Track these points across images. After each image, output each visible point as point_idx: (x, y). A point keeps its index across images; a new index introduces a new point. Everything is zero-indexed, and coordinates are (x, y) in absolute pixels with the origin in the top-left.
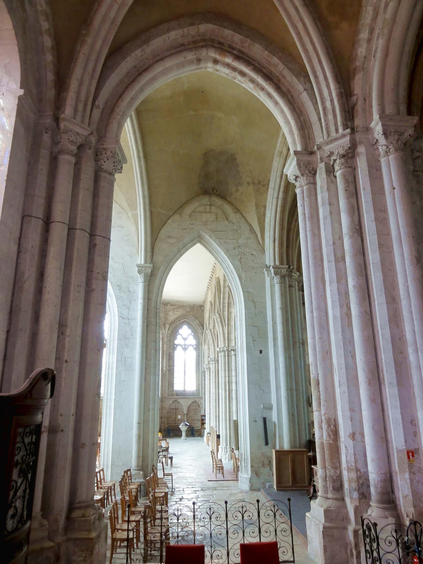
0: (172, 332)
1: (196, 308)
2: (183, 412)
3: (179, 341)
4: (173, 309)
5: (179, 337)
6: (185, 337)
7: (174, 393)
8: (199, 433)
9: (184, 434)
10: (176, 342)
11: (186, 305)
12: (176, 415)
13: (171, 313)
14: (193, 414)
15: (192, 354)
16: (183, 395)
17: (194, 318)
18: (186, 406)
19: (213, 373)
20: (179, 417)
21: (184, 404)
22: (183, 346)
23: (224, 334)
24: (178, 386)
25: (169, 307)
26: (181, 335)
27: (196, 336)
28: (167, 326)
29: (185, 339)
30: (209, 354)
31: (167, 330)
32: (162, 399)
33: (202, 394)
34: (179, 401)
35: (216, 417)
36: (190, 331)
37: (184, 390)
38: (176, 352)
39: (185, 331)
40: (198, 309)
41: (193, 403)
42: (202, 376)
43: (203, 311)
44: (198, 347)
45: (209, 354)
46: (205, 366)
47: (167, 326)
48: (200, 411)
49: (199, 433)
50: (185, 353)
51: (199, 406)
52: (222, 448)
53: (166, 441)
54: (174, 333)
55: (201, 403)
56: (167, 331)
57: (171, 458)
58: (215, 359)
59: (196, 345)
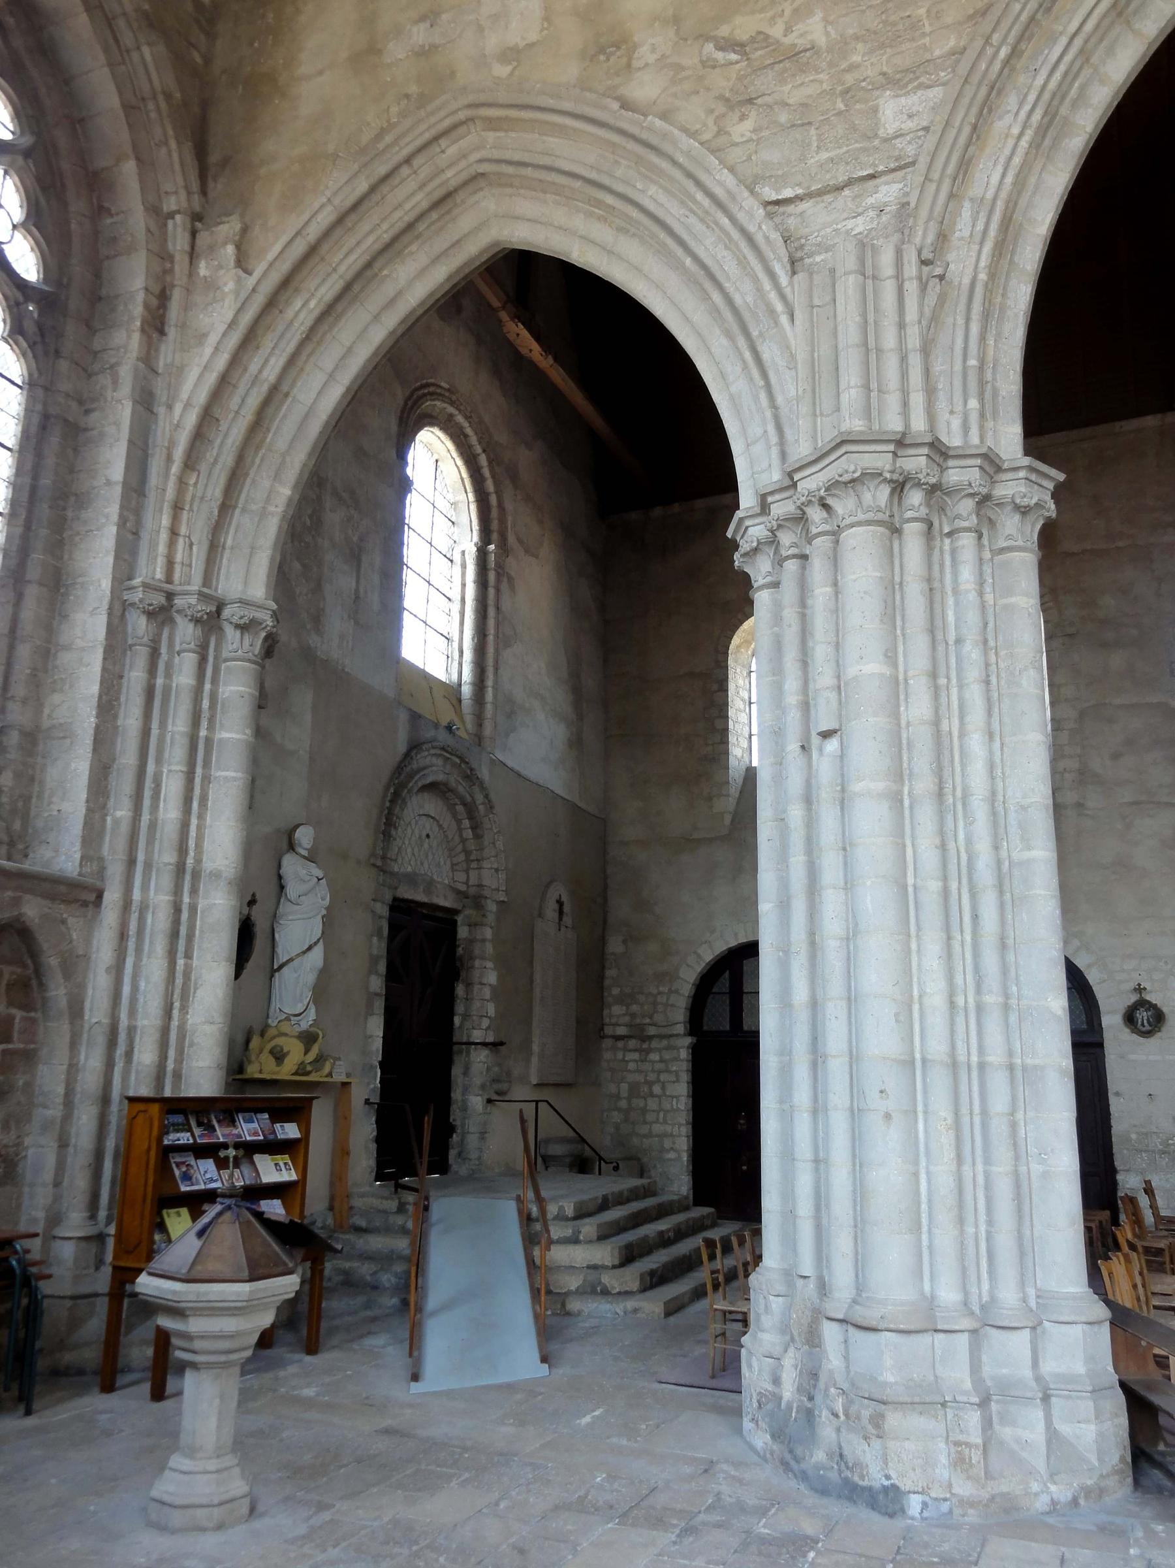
48: (29, 1057)
55: (74, 965)
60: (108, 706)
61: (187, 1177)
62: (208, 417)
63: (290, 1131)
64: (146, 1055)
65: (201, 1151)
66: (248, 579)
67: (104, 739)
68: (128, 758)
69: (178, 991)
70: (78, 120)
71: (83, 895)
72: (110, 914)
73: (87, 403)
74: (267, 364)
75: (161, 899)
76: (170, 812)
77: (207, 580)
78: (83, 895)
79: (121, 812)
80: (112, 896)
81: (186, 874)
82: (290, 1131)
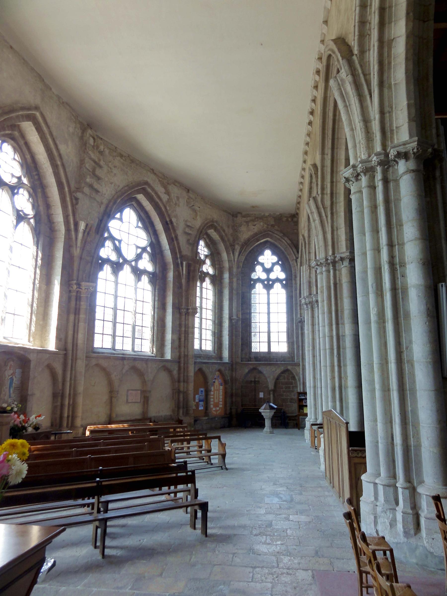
0: (246, 259)
1: (284, 219)
2: (267, 387)
5: (259, 268)
6: (268, 266)
7: (252, 356)
8: (295, 422)
9: (268, 423)
10: (254, 276)
11: (267, 214)
12: (256, 391)
13: (243, 228)
14: (284, 392)
15: (279, 294)
17: (282, 235)
18: (272, 377)
19: (322, 292)
20: (261, 395)
21: (270, 374)
22: (266, 282)
23: (366, 121)
24: (259, 346)
25: (239, 219)
26: (262, 265)
27: (286, 266)
28: (238, 248)
29: (268, 271)
31: (237, 254)
32: (232, 365)
33: (298, 358)
35: (333, 389)
36: (275, 259)
37: (269, 352)
39: (268, 258)
40: (287, 220)
42: (297, 329)
43: (296, 223)
44: (290, 284)
45: (310, 277)
46: (303, 301)
47: (238, 248)
48: (296, 387)
49: (295, 422)
50: (268, 294)
51: (294, 378)
52: (375, 484)
53: (220, 440)
54: (250, 262)
55: (298, 374)
57: (204, 506)
58: (327, 260)
60: (297, 337)
70: (283, 253)
72: (301, 367)
79: (300, 352)
80: (301, 364)
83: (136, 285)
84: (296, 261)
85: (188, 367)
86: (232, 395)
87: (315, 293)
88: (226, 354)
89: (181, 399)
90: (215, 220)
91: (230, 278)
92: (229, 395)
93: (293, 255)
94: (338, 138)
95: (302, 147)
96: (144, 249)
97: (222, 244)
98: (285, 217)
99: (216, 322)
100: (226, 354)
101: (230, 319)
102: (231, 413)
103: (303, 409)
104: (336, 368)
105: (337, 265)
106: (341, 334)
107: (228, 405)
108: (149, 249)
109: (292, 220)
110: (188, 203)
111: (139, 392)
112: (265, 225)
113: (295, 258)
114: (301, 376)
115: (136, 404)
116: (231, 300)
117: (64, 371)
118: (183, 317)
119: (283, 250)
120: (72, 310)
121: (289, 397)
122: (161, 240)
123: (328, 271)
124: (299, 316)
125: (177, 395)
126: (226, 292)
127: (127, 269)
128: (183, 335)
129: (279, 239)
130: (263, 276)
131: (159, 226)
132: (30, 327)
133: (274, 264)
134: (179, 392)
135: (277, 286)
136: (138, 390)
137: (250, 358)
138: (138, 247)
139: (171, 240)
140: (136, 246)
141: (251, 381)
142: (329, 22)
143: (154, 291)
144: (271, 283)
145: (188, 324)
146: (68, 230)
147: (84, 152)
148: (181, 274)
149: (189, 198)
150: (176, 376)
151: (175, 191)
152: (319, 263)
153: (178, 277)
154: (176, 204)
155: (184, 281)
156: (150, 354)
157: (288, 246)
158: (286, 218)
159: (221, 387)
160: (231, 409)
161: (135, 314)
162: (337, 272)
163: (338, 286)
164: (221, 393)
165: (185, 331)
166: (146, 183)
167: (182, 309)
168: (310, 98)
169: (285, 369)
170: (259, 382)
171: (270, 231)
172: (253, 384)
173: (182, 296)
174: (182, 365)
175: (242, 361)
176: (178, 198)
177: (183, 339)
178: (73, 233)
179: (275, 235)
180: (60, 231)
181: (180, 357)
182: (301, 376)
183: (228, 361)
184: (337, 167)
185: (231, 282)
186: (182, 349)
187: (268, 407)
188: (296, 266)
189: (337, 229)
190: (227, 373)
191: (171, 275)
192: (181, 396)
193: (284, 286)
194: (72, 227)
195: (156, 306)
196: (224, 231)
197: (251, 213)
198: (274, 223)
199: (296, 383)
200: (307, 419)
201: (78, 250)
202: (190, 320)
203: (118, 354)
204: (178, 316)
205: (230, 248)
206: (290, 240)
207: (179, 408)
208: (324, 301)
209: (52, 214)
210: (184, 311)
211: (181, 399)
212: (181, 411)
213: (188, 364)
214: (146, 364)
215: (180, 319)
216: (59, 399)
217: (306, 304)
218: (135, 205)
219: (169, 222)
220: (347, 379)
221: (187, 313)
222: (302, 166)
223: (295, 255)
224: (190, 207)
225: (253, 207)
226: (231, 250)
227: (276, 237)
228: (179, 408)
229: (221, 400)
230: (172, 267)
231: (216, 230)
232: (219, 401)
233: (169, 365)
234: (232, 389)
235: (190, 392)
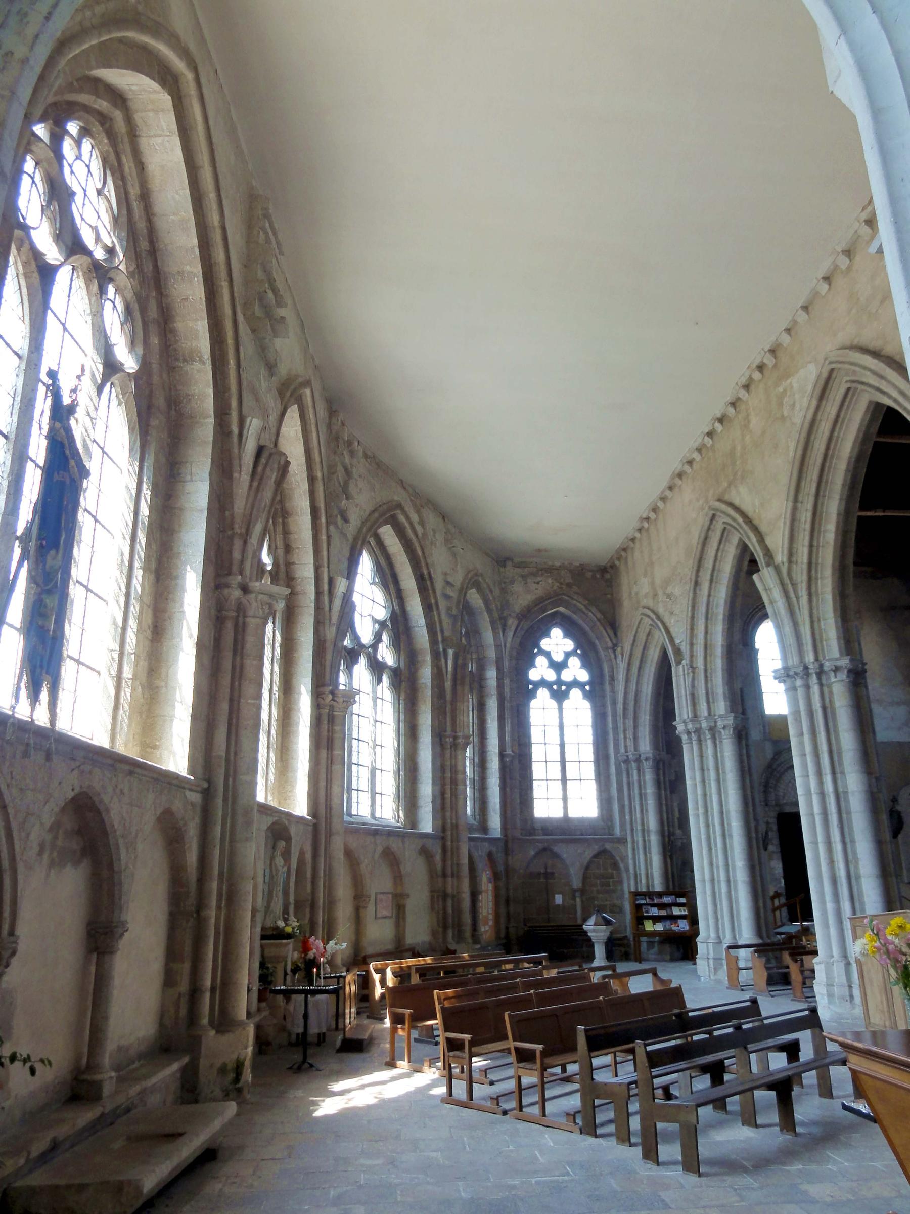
0: (521, 644)
1: (589, 575)
3: (540, 671)
4: (523, 576)
5: (541, 661)
6: (558, 657)
8: (623, 950)
10: (534, 675)
11: (557, 564)
12: (549, 893)
13: (518, 587)
14: (598, 892)
15: (579, 708)
16: (566, 831)
17: (586, 603)
20: (559, 899)
21: (574, 860)
24: (546, 805)
25: (510, 571)
26: (547, 654)
28: (512, 623)
29: (558, 667)
30: (693, 686)
31: (511, 634)
32: (506, 842)
34: (556, 849)
36: (569, 645)
38: (533, 703)
39: (556, 642)
40: (594, 577)
41: (596, 856)
44: (596, 692)
45: (693, 686)
47: (512, 623)
48: (621, 882)
49: (623, 950)
51: (615, 866)
53: (655, 974)
54: (526, 649)
55: (624, 858)
56: (509, 640)
58: (806, 668)
59: (590, 683)
60: (620, 790)
61: (647, 912)
62: (625, 703)
63: (683, 900)
64: (644, 881)
65: (653, 905)
66: (646, 746)
67: (621, 799)
68: (627, 803)
69: (648, 863)
70: (584, 633)
71: (622, 841)
72: (630, 845)
73: (604, 706)
74: (633, 686)
75: (640, 839)
76: (638, 816)
77: (636, 750)
78: (622, 841)
79: (627, 817)
80: (629, 839)
81: (645, 831)
82: (683, 900)
83: (374, 691)
84: (614, 651)
85: (458, 848)
86: (507, 902)
87: (706, 714)
88: (495, 822)
89: (450, 910)
90: (480, 571)
91: (500, 679)
92: (502, 900)
93: (608, 640)
94: (827, 482)
95: (676, 465)
96: (382, 624)
97: (486, 617)
98: (591, 571)
99: (476, 760)
100: (495, 822)
101: (502, 755)
102: (507, 936)
103: (643, 924)
104: (838, 847)
105: (824, 677)
106: (841, 789)
107: (503, 920)
108: (389, 623)
109: (603, 576)
110: (447, 541)
111: (390, 896)
112: (557, 584)
113: (610, 644)
114: (631, 862)
115: (387, 921)
116: (501, 719)
117: (315, 856)
118: (448, 752)
119: (587, 628)
120: (324, 742)
121: (608, 903)
122: (408, 608)
123: (807, 687)
124: (622, 750)
125: (441, 903)
126: (492, 705)
127: (363, 660)
128: (448, 787)
129: (581, 610)
130: (551, 676)
131: (409, 583)
132: (267, 774)
133: (568, 655)
134: (445, 896)
135: (576, 694)
136: (388, 893)
137: (534, 829)
138: (375, 621)
139: (428, 608)
140: (373, 617)
141: (539, 874)
142: (810, 308)
143: (397, 702)
144: (563, 688)
145: (456, 766)
146: (318, 593)
147: (335, 453)
148: (444, 670)
149: (448, 532)
150: (439, 867)
151: (432, 520)
152: (791, 673)
153: (438, 675)
154: (432, 543)
155: (448, 685)
156: (393, 822)
157: (598, 623)
158: (590, 573)
159: (490, 885)
160: (507, 928)
161: (374, 748)
162: (826, 690)
163: (829, 710)
164: (491, 898)
165: (451, 778)
166: (399, 506)
167: (446, 737)
168: (729, 398)
169: (602, 849)
170: (553, 873)
171: (565, 595)
172: (542, 880)
173: (445, 713)
174: (449, 843)
175: (522, 835)
176: (434, 531)
177: (448, 795)
178: (326, 599)
179: (575, 602)
180: (305, 593)
181: (444, 829)
182: (631, 862)
183: (499, 836)
184: (820, 525)
185: (500, 686)
186: (448, 814)
187: (601, 920)
188: (613, 660)
189: (819, 620)
190: (499, 857)
191: (426, 674)
192: (449, 903)
193: (588, 695)
194: (326, 587)
195: (402, 731)
196: (491, 591)
197: (532, 560)
198: (571, 581)
199: (619, 874)
200: (698, 939)
201: (334, 629)
202: (460, 757)
203: (358, 823)
204: (438, 749)
205: (499, 623)
206: (600, 611)
207: (445, 928)
208: (802, 734)
209: (293, 563)
210: (449, 740)
211: (450, 910)
212: (450, 933)
213: (458, 841)
214: (403, 842)
215: (442, 755)
216: (308, 910)
217: (689, 733)
218: (373, 543)
219: (427, 577)
220: (857, 863)
221: (454, 746)
222: (662, 492)
223: (611, 640)
224: (450, 549)
225: (539, 551)
226: (500, 626)
227: (575, 606)
228: (445, 928)
229: (490, 911)
230: (428, 658)
231: (479, 590)
232: (488, 913)
233: (429, 843)
234: (507, 889)
235: (464, 895)
